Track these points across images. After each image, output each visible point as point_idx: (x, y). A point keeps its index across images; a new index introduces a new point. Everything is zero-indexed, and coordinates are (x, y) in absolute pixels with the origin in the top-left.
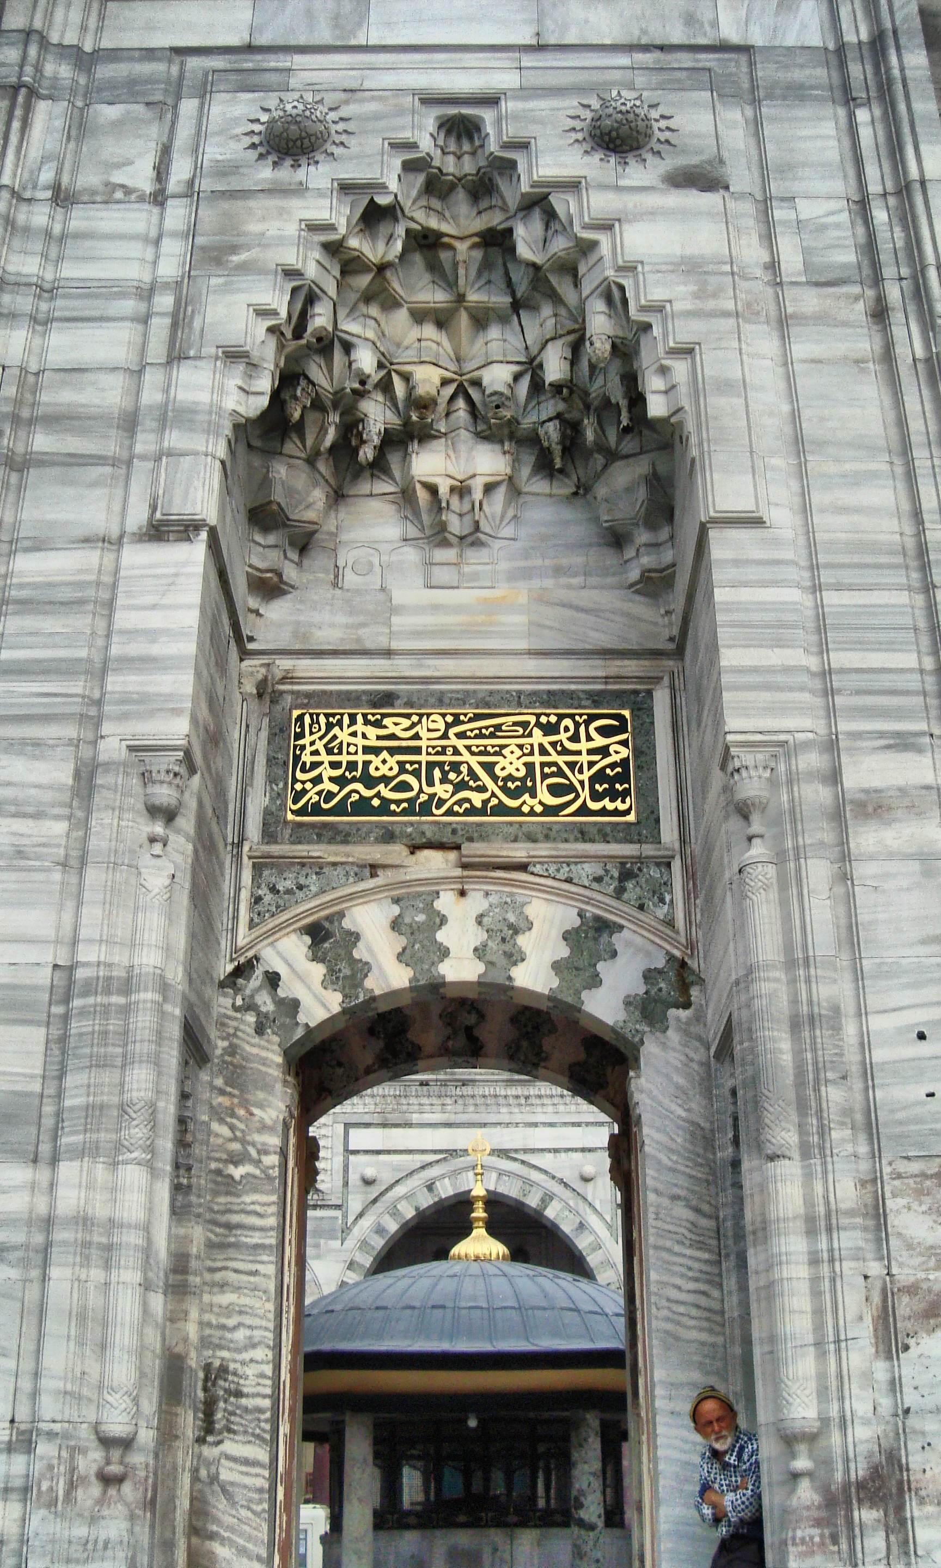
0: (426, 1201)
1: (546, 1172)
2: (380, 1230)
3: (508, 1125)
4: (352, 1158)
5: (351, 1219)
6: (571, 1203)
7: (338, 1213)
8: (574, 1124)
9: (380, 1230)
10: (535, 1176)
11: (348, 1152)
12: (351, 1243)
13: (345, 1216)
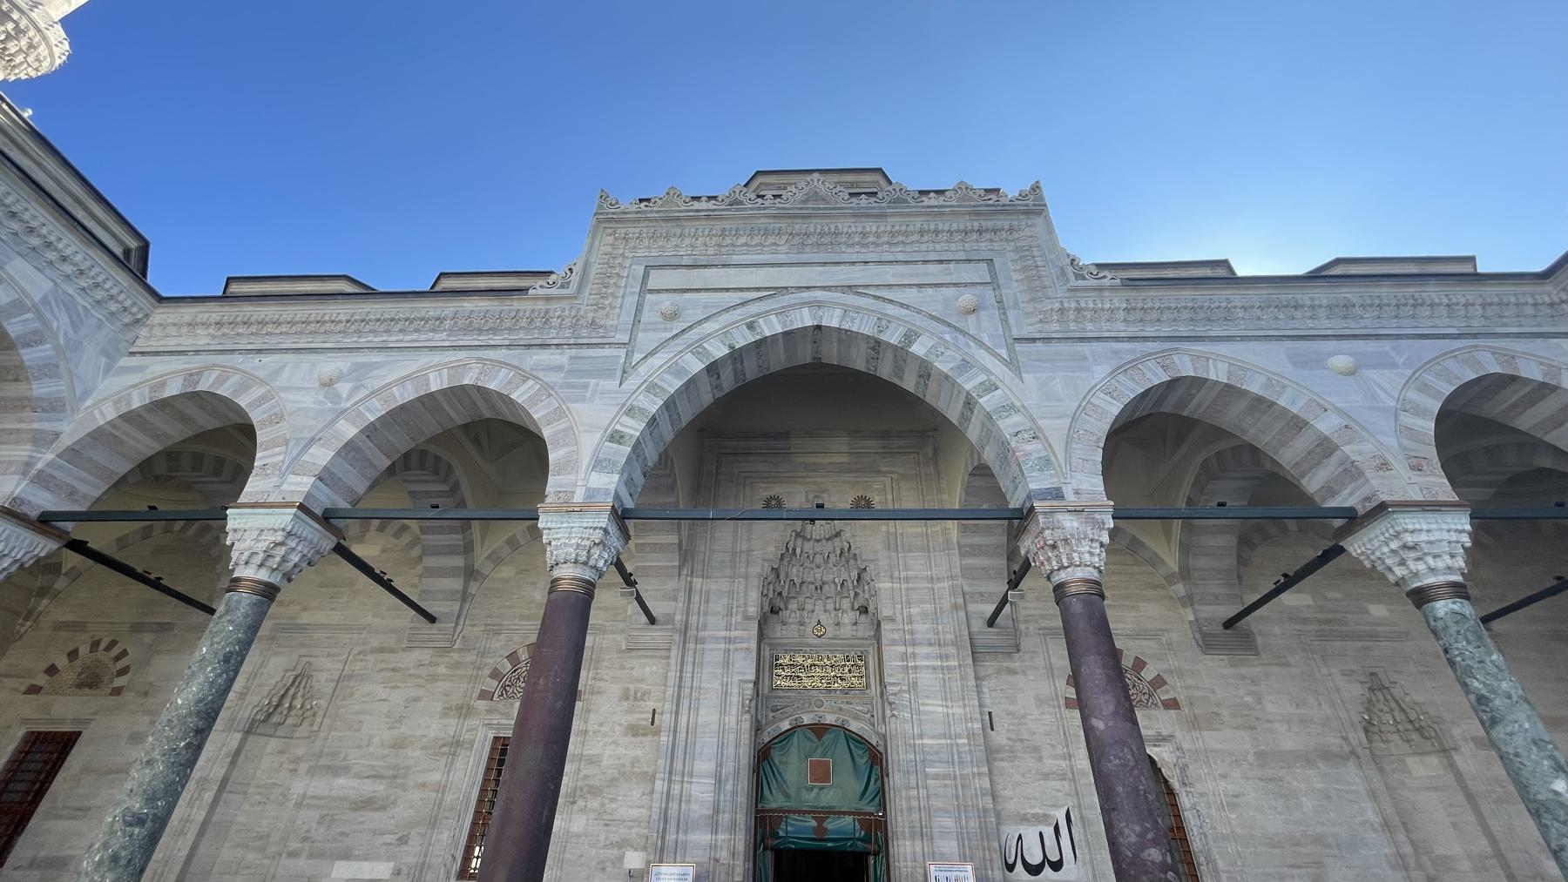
0: (743, 339)
1: (907, 307)
2: (676, 371)
3: (853, 263)
4: (648, 296)
5: (637, 357)
6: (947, 337)
7: (622, 352)
8: (941, 262)
9: (676, 371)
10: (891, 310)
11: (644, 290)
12: (632, 382)
13: (628, 355)
